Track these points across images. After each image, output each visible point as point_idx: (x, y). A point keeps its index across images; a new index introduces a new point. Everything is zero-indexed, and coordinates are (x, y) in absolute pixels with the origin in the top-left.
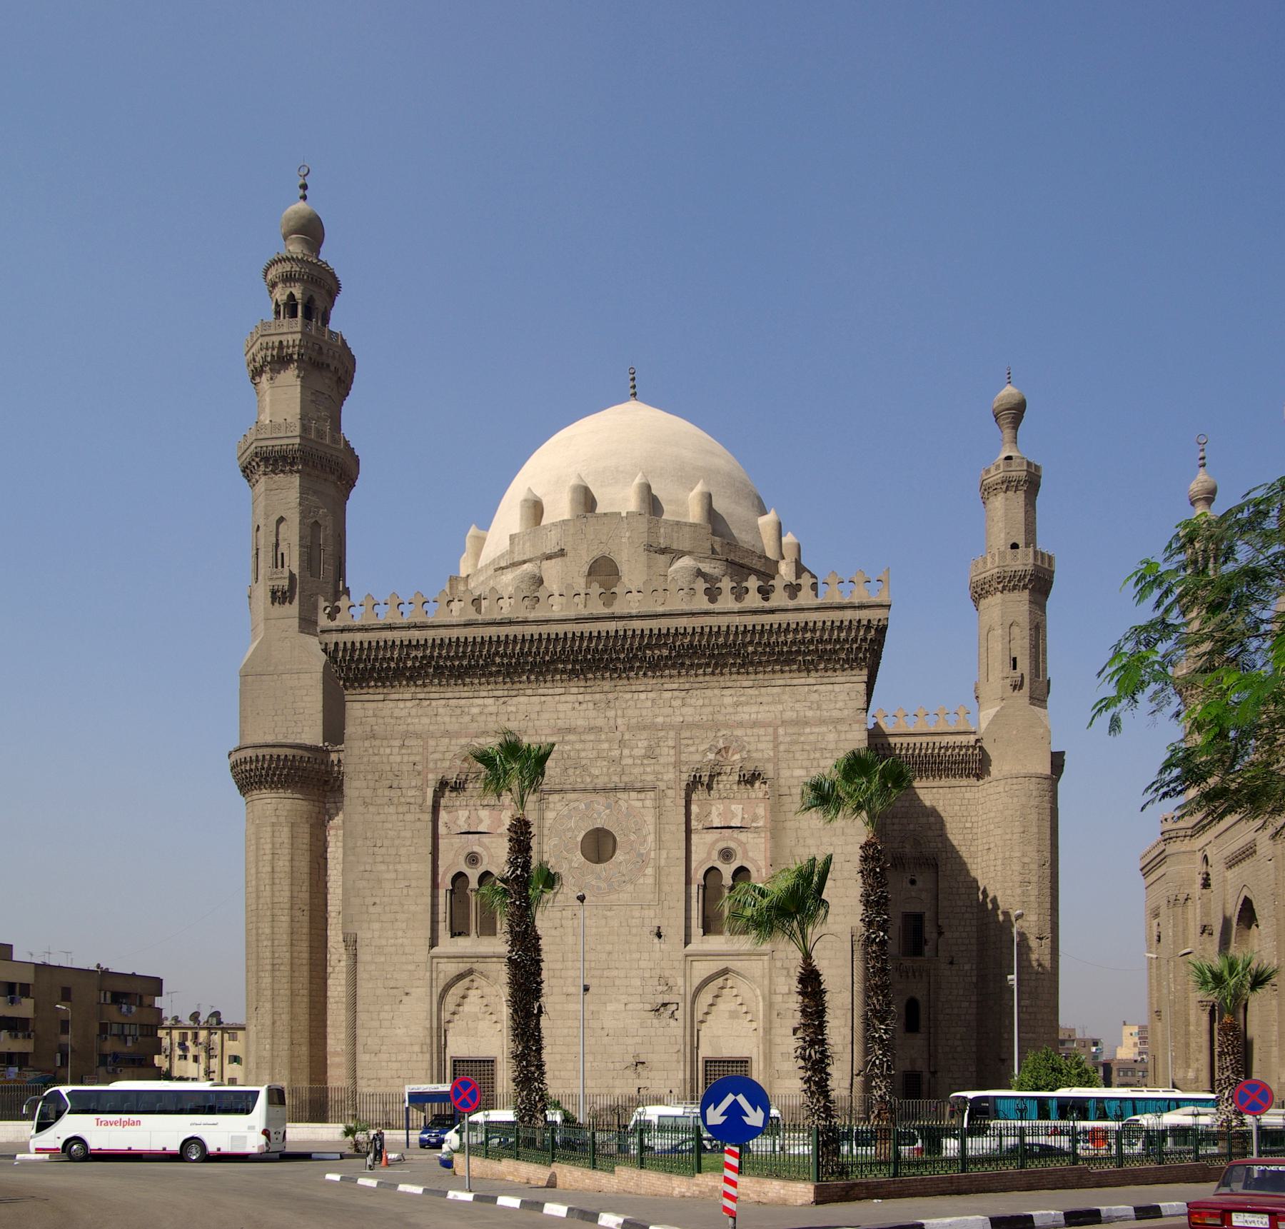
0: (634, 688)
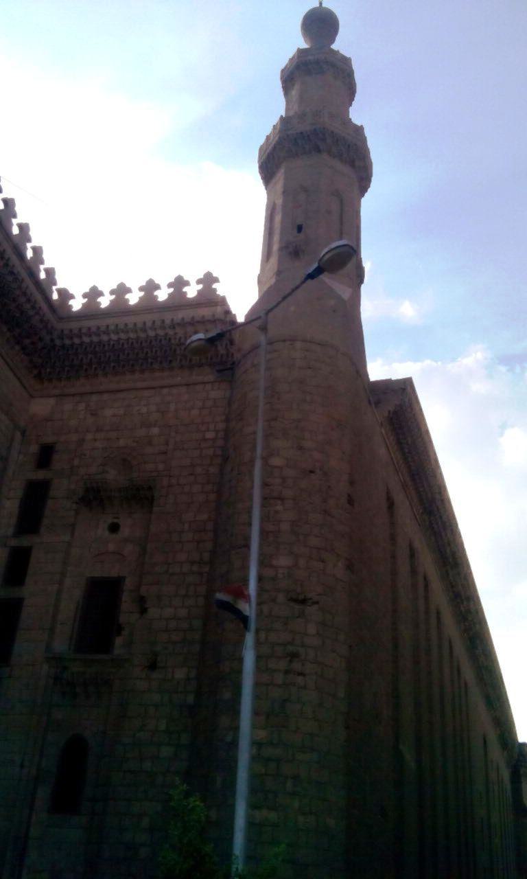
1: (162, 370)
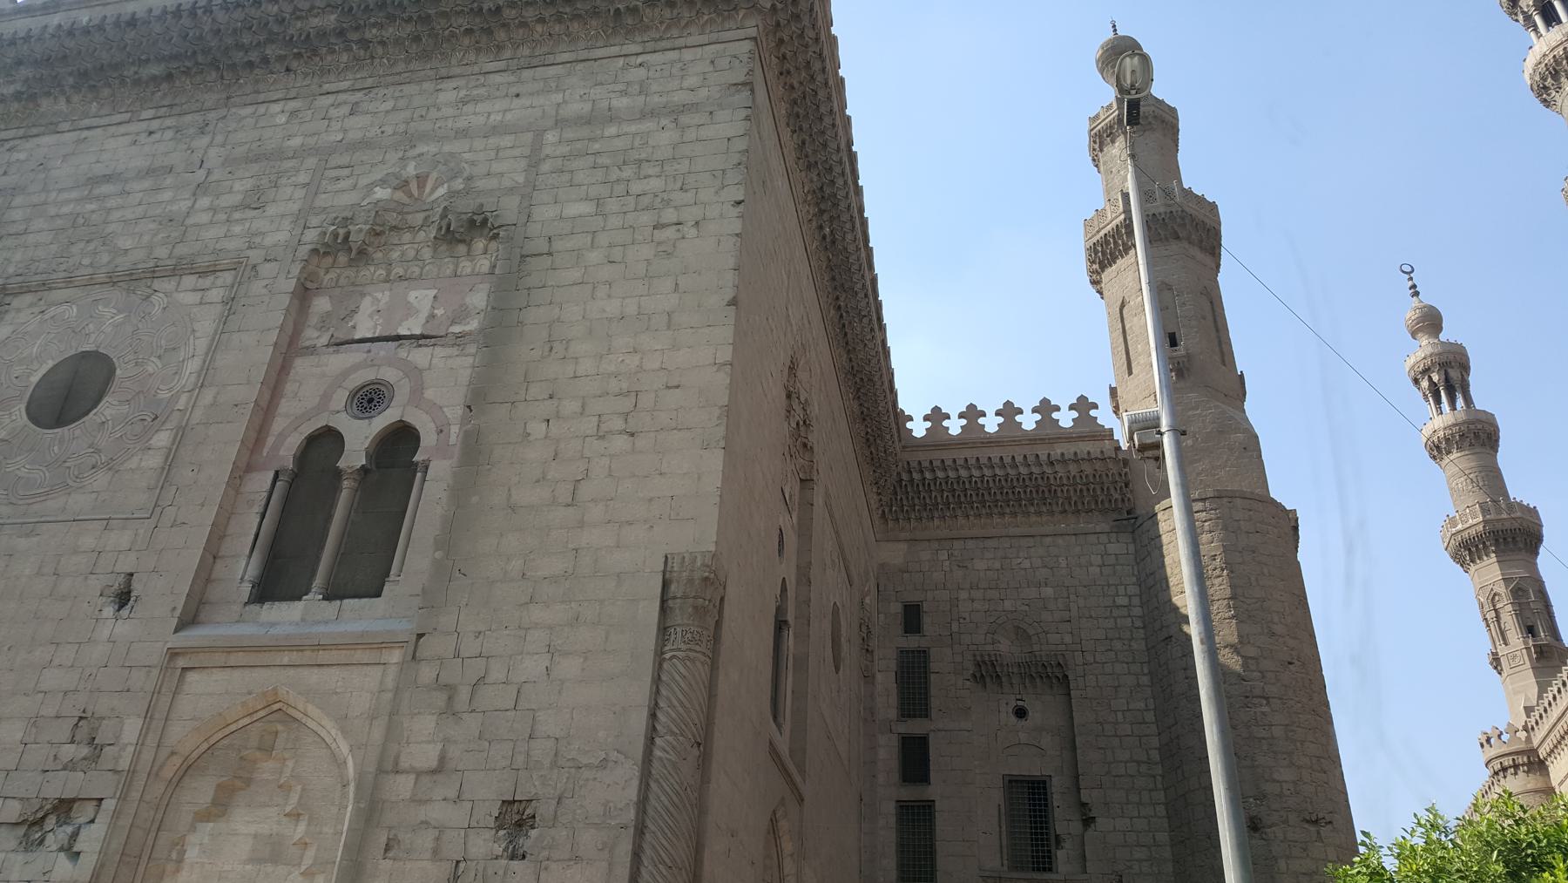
0: (262, 97)
1: (1039, 514)
